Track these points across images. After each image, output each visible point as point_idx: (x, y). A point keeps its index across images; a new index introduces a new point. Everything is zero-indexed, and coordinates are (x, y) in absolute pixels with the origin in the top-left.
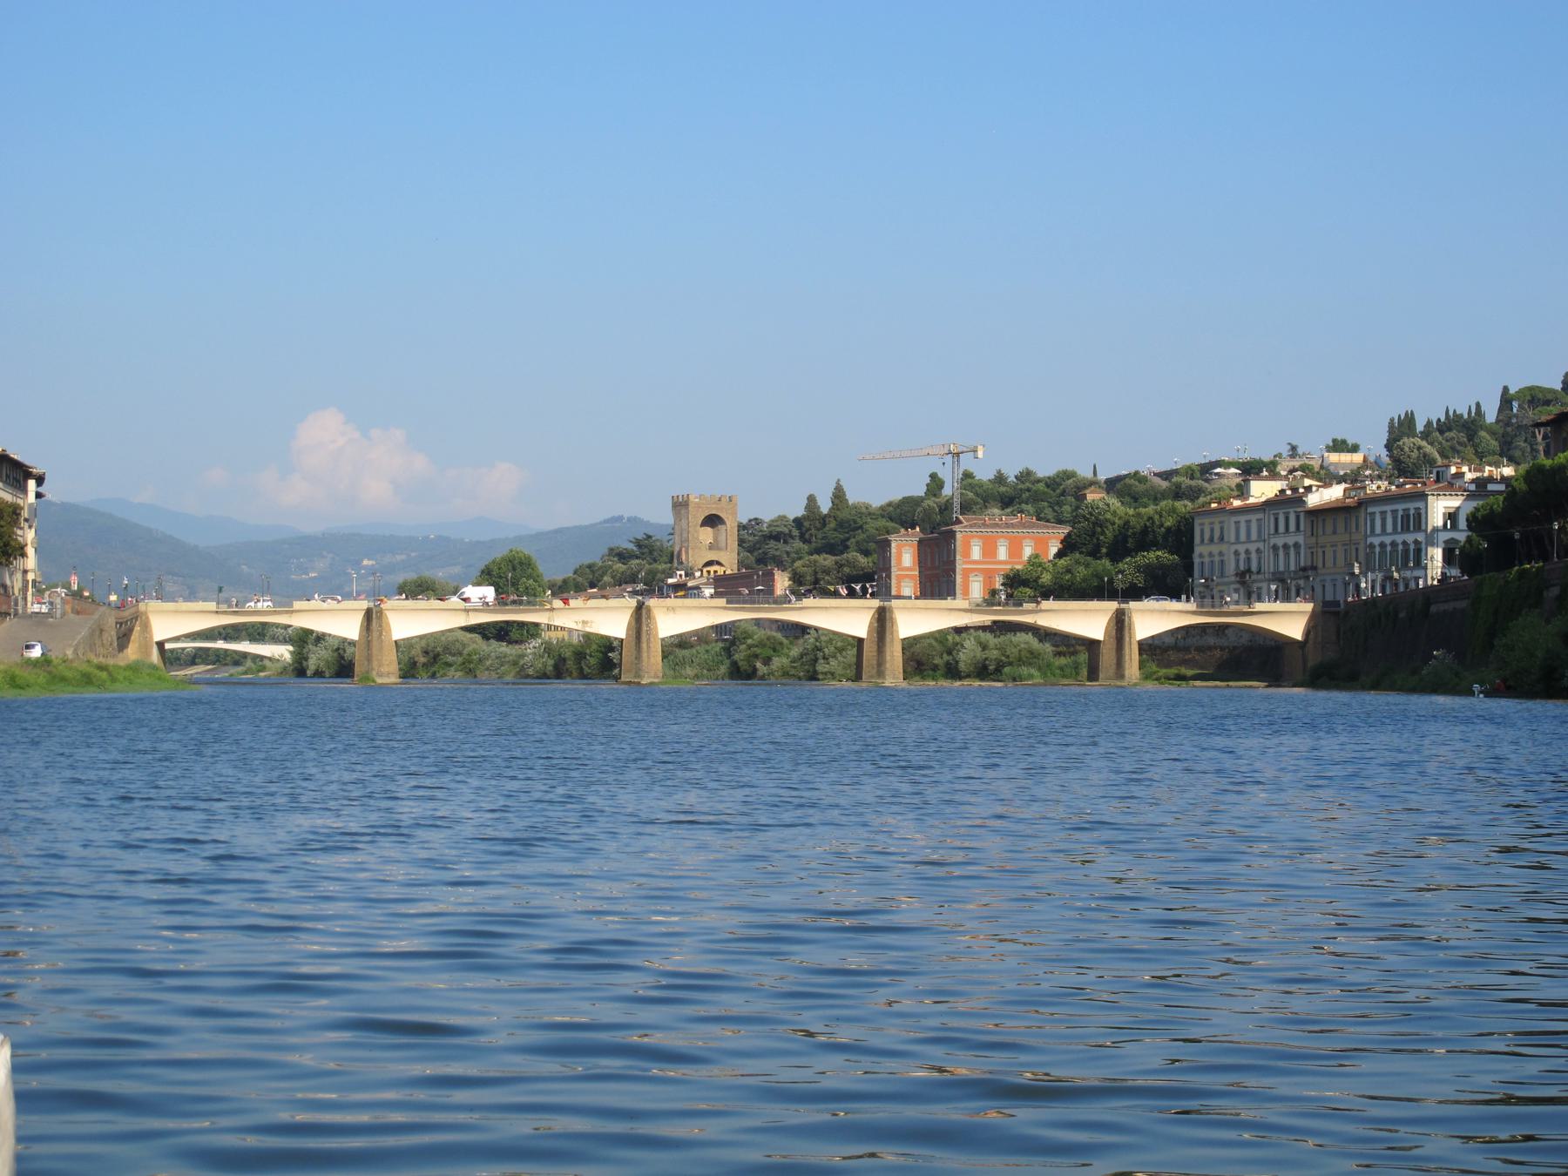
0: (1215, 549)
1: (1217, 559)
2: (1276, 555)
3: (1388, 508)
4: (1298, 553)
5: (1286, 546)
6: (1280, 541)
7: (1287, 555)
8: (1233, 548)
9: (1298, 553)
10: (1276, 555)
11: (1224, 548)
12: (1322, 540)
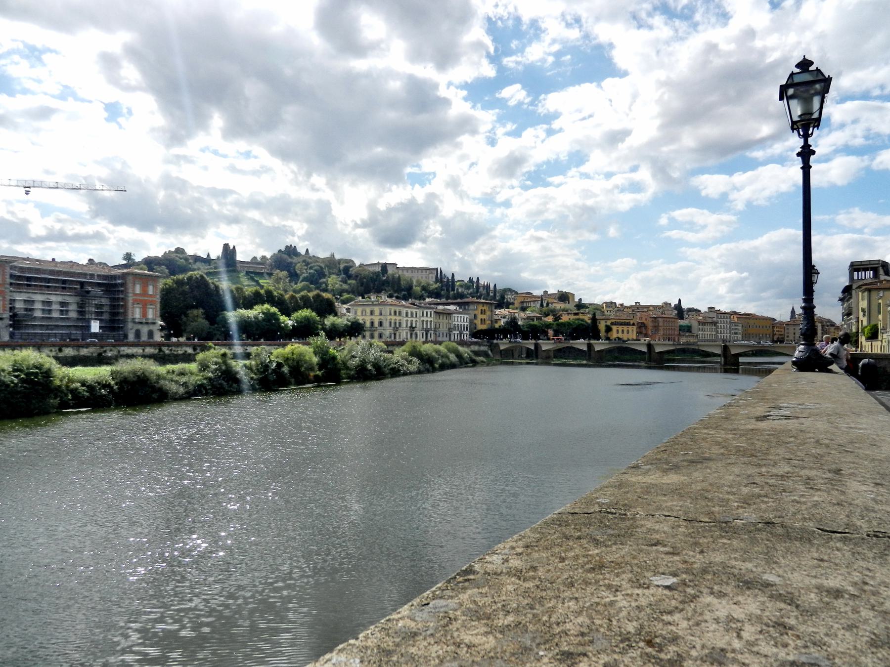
0: (398, 318)
1: (398, 322)
2: (423, 324)
3: (459, 316)
4: (431, 324)
5: (427, 321)
6: (425, 319)
7: (427, 324)
8: (406, 319)
9: (431, 324)
10: (423, 324)
11: (401, 318)
12: (439, 321)
